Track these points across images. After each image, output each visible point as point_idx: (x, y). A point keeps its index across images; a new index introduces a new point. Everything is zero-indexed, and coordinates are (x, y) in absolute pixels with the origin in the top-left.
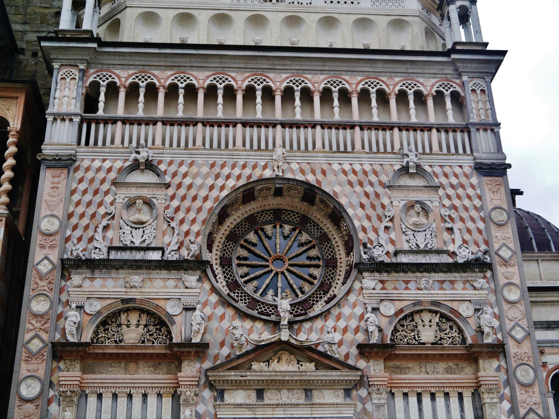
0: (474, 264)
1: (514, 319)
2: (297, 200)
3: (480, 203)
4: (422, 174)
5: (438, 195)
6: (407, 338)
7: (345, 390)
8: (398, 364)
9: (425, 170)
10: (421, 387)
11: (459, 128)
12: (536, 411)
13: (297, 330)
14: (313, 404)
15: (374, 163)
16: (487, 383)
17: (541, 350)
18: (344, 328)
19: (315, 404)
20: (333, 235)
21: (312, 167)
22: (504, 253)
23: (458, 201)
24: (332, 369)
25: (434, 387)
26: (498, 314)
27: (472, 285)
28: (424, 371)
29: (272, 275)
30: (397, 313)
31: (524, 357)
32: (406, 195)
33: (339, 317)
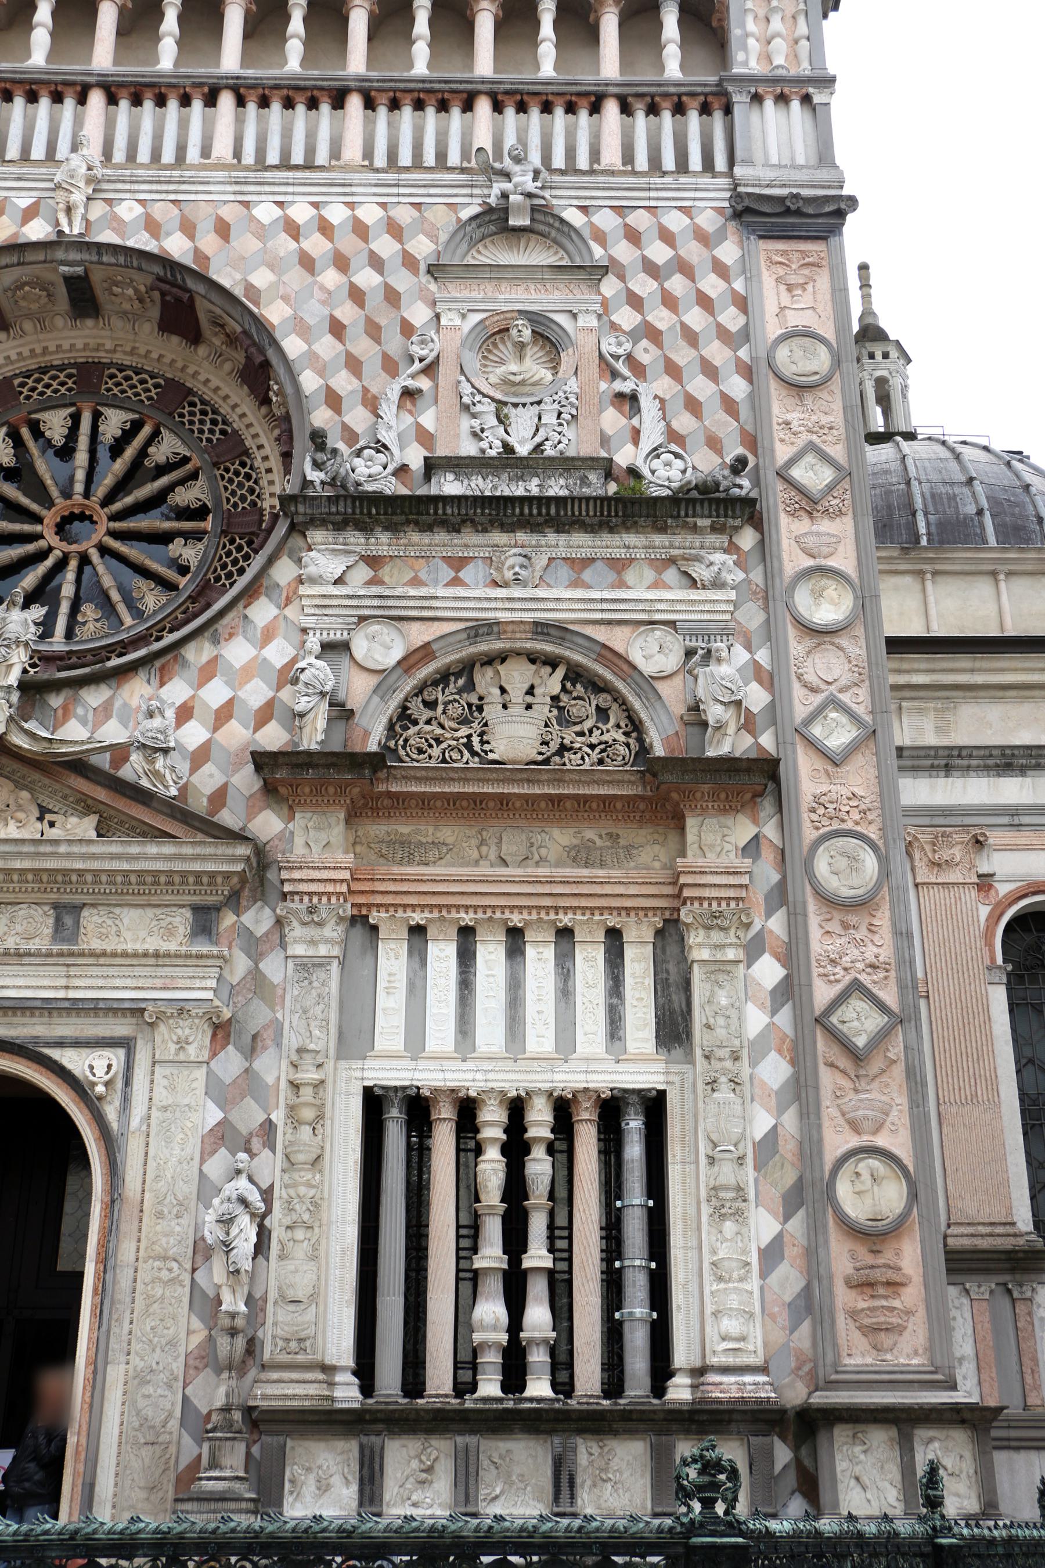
0: (694, 501)
1: (823, 686)
2: (147, 327)
3: (742, 320)
4: (553, 233)
5: (600, 294)
6: (444, 745)
7: (196, 909)
8: (404, 829)
9: (562, 221)
10: (476, 908)
11: (693, 95)
12: (875, 991)
13: (60, 712)
14: (71, 954)
15: (395, 199)
16: (707, 893)
17: (975, 836)
18: (222, 707)
19: (82, 954)
20: (256, 436)
21: (186, 211)
22: (811, 473)
23: (665, 313)
24: (144, 834)
25: (520, 908)
26: (769, 668)
27: (686, 573)
28: (492, 856)
29: (49, 562)
30: (412, 661)
31: (847, 808)
32: (490, 294)
33: (208, 672)
